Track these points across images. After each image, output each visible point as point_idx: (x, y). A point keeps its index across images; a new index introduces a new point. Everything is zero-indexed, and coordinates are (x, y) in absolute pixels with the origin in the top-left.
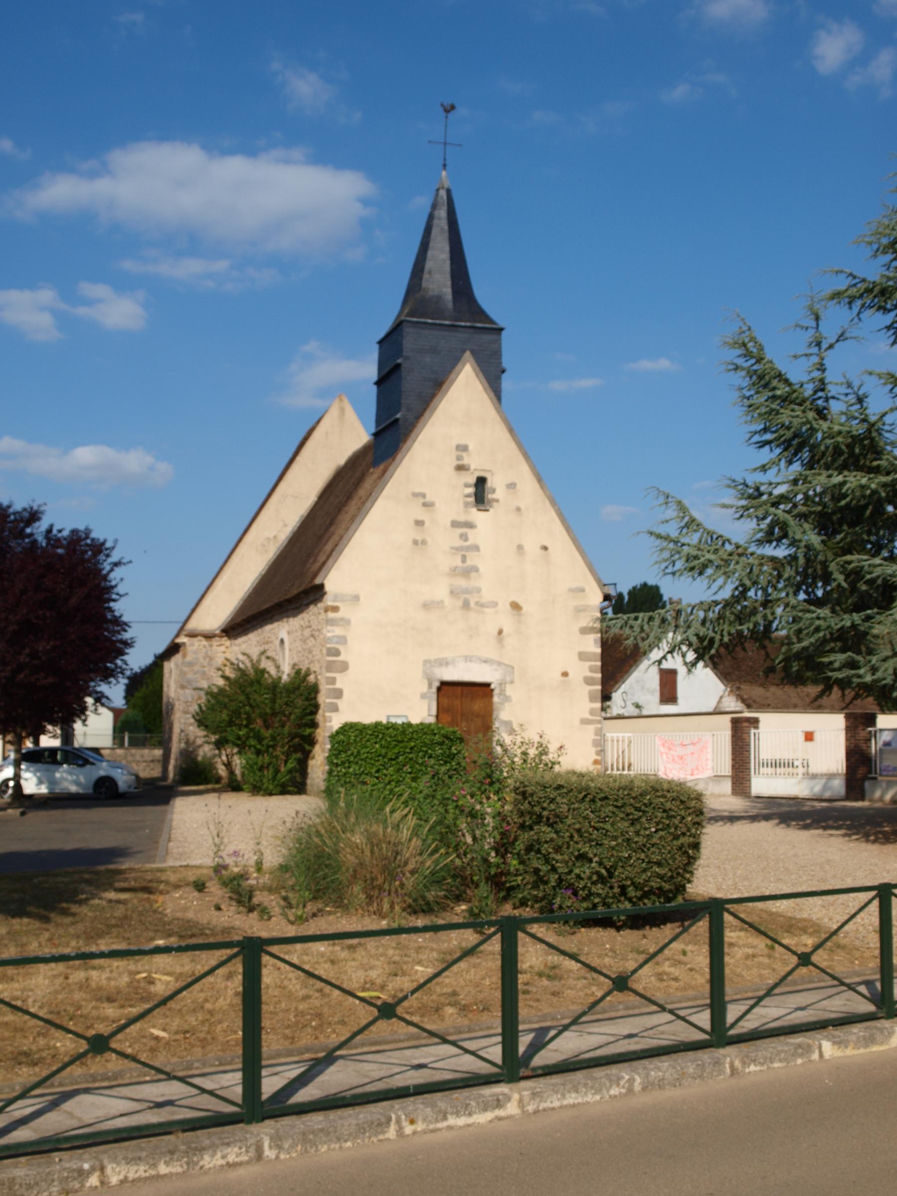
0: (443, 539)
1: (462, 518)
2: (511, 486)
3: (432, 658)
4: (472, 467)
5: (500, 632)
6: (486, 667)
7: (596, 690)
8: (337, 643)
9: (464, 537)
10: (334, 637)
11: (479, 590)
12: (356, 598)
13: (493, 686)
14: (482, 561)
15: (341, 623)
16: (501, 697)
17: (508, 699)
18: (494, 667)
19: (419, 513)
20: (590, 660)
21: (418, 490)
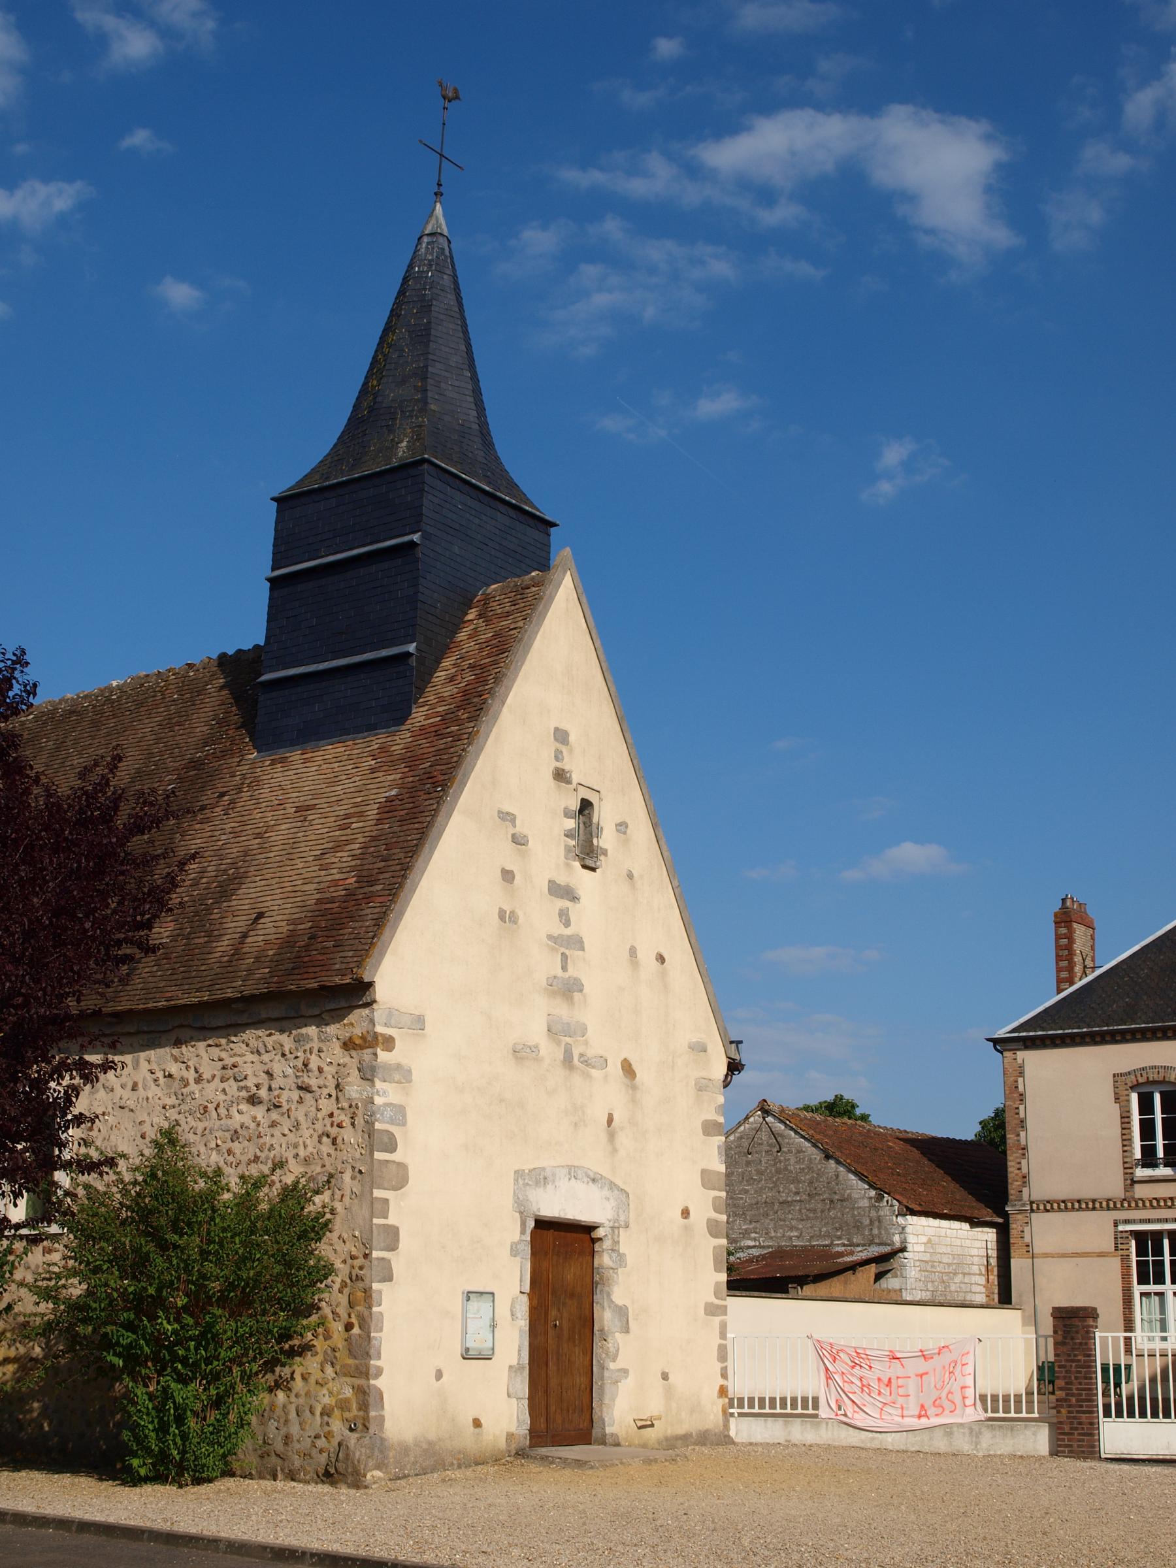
0: (540, 916)
1: (562, 880)
2: (622, 827)
3: (527, 1167)
4: (575, 779)
5: (610, 1120)
6: (596, 1192)
7: (721, 1247)
8: (392, 1122)
9: (564, 918)
10: (386, 1105)
11: (584, 1030)
12: (419, 1023)
13: (600, 1233)
14: (596, 972)
15: (397, 1077)
16: (614, 1255)
17: (621, 1258)
18: (606, 1192)
19: (507, 857)
20: (714, 1189)
21: (507, 808)
